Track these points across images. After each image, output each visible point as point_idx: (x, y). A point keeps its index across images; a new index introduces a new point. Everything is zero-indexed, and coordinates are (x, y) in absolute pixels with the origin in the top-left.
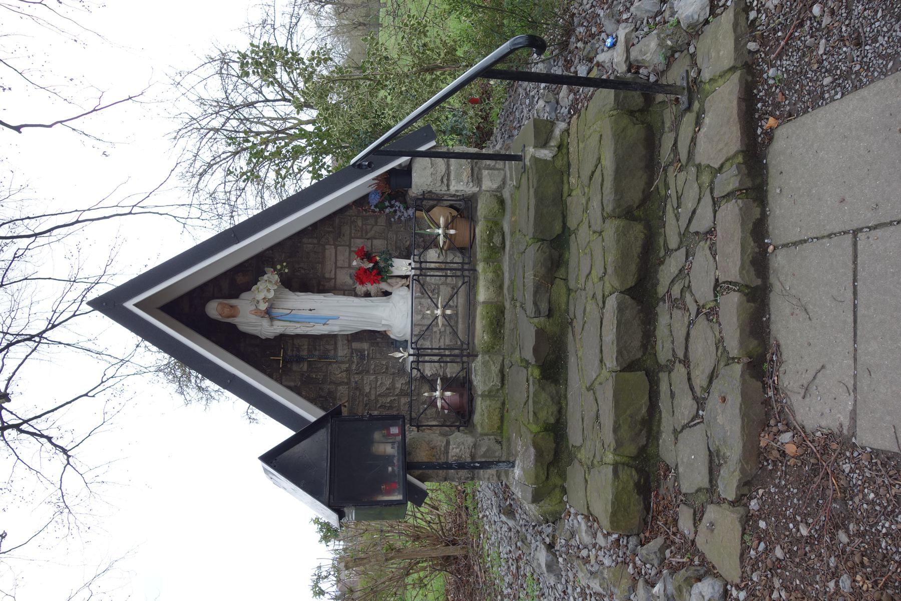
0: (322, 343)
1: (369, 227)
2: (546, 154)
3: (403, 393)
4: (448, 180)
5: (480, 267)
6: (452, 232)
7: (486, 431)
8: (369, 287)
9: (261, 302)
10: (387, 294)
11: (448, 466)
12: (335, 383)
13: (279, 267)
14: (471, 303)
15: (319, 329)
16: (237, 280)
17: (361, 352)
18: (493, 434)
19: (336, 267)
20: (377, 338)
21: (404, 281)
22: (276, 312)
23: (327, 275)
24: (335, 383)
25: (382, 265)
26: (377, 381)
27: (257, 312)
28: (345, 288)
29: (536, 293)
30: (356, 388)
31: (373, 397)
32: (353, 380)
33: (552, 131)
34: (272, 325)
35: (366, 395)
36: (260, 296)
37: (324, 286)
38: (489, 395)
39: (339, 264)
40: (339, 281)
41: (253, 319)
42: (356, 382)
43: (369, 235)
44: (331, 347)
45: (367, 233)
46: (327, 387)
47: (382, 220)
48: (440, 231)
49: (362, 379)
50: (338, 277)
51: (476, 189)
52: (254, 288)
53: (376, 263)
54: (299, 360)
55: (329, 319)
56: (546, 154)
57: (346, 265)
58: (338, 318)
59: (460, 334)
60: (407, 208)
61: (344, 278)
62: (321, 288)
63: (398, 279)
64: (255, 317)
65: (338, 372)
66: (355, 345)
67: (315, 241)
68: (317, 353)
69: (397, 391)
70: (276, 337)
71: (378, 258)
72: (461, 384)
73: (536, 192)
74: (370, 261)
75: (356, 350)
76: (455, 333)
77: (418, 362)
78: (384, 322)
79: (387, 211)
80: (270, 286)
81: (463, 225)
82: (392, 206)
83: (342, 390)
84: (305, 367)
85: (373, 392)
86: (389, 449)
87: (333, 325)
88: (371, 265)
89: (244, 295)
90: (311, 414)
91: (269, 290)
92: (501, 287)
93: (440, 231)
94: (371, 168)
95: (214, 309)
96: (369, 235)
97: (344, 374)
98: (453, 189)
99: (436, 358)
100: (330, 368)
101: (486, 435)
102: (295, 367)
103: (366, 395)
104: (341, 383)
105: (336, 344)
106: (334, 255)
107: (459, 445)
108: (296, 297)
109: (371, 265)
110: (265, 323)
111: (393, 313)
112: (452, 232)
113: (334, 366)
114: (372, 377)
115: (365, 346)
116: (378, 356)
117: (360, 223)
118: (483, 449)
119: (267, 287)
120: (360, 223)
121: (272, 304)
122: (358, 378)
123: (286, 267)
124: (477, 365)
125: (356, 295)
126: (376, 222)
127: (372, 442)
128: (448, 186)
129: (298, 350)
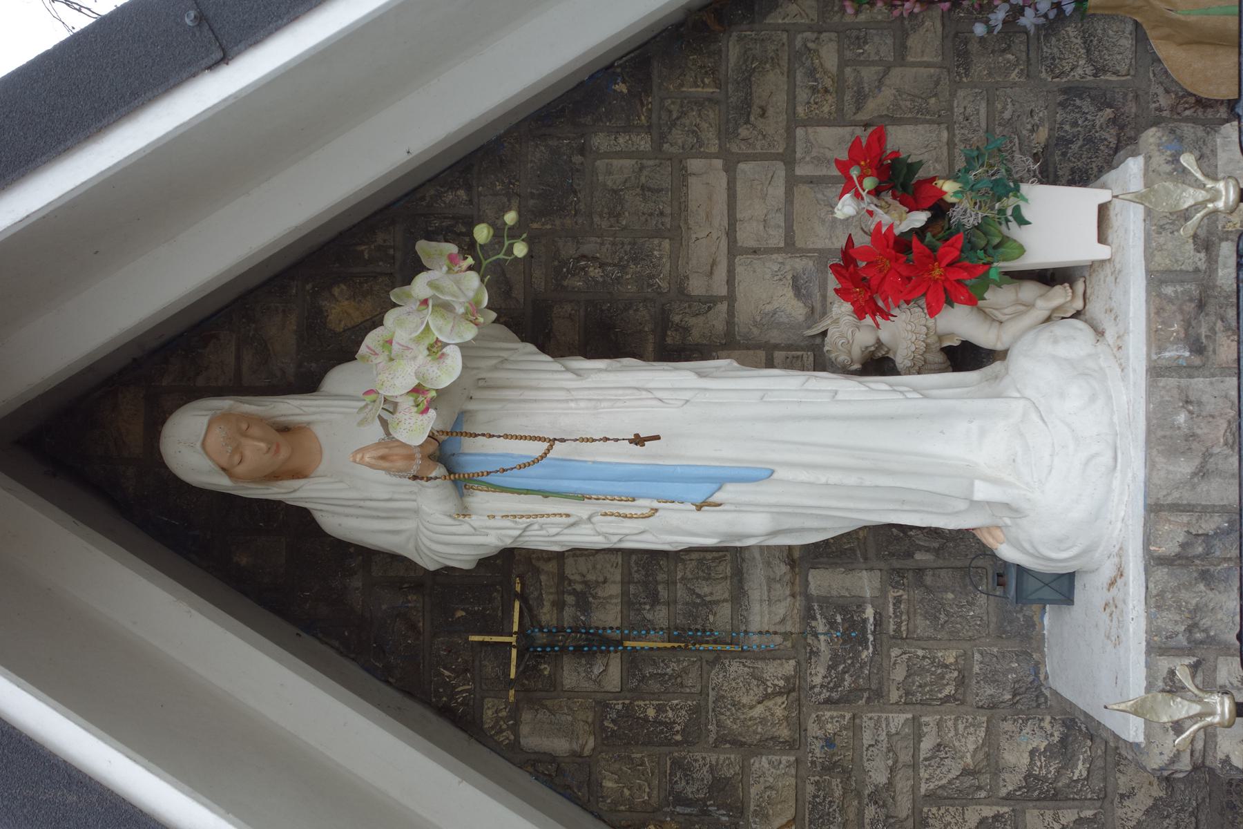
0: (685, 590)
1: (869, 74)
8: (905, 328)
9: (407, 403)
10: (964, 356)
12: (737, 744)
13: (482, 233)
15: (677, 527)
16: (298, 314)
17: (846, 614)
21: (1059, 295)
22: (481, 451)
23: (696, 286)
24: (737, 744)
25: (967, 213)
26: (918, 737)
27: (388, 454)
28: (775, 336)
31: (903, 807)
32: (813, 729)
34: (464, 512)
35: (875, 798)
37: (686, 330)
39: (746, 236)
41: (381, 485)
42: (829, 742)
43: (872, 108)
44: (720, 591)
45: (860, 99)
49: (855, 727)
50: (740, 290)
52: (372, 339)
53: (940, 209)
54: (593, 644)
55: (721, 482)
57: (776, 238)
58: (763, 475)
61: (766, 293)
62: (672, 338)
63: (1029, 290)
64: (381, 475)
65: (749, 697)
66: (821, 581)
67: (643, 143)
68: (660, 616)
69: (1011, 782)
70: (484, 563)
71: (949, 187)
74: (913, 205)
75: (825, 601)
78: (982, 492)
80: (442, 329)
83: (771, 775)
84: (612, 673)
85: (903, 785)
87: (740, 507)
88: (919, 218)
89: (340, 378)
91: (436, 349)
95: (197, 444)
96: (872, 108)
97: (778, 707)
100: (716, 677)
102: (571, 675)
103: (875, 798)
104: (766, 745)
106: (721, 197)
108: (568, 380)
109: (919, 218)
113: (735, 668)
114: (898, 720)
116: (922, 625)
117: (829, 57)
119: (427, 333)
120: (829, 57)
121: (462, 416)
122: (834, 720)
123: (514, 233)
126: (901, 50)
129: (583, 603)
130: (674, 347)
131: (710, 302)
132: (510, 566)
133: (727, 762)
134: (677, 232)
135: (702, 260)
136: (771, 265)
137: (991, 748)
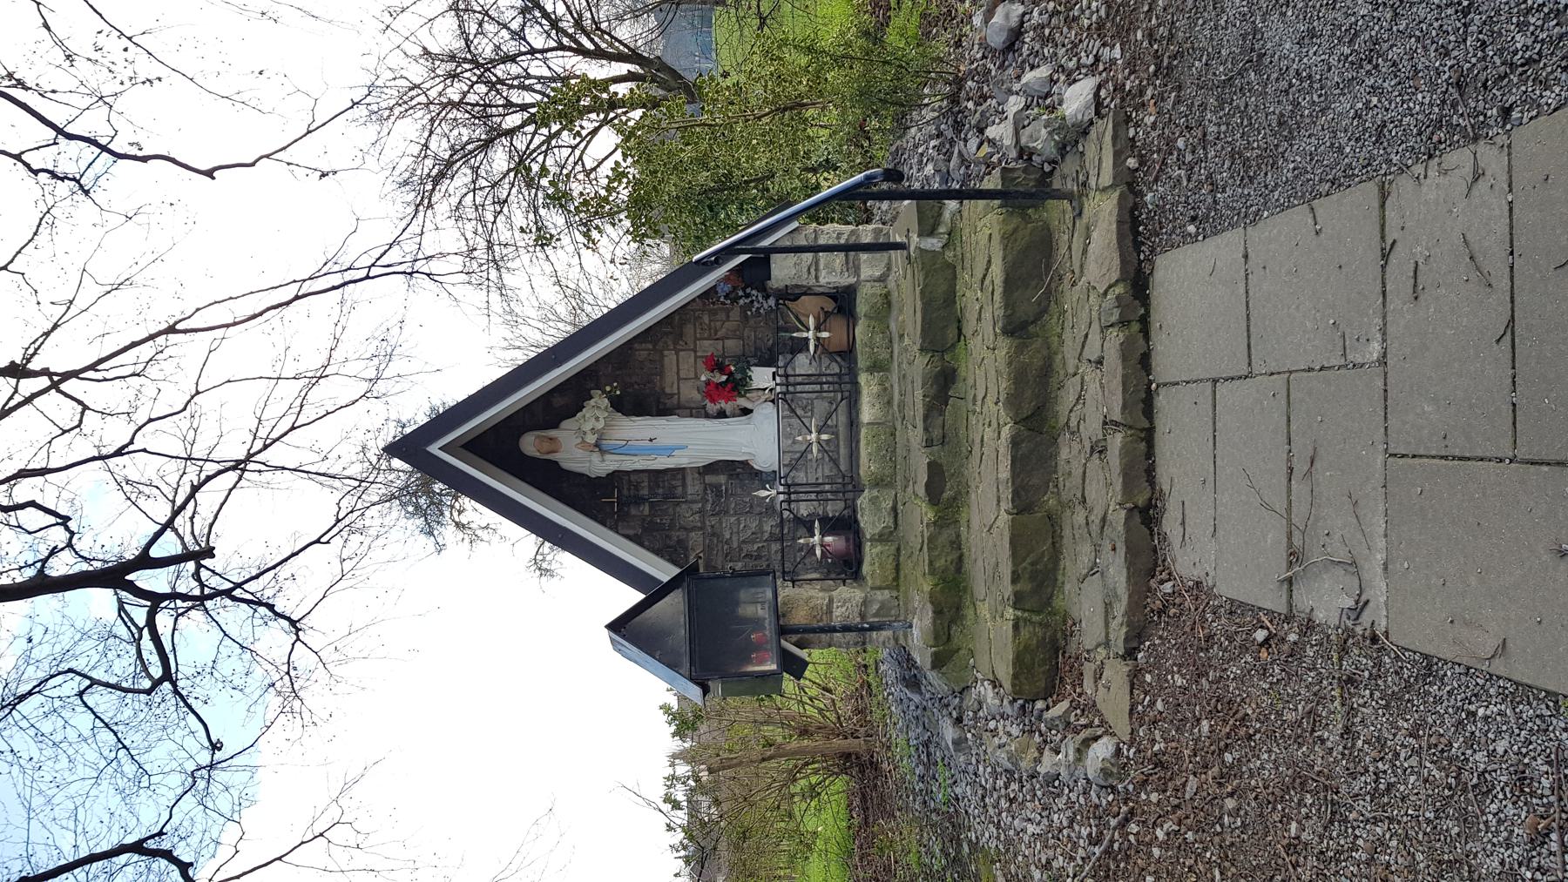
0: (666, 481)
2: (933, 243)
3: (773, 538)
4: (817, 270)
5: (863, 378)
6: (825, 335)
7: (878, 583)
10: (746, 412)
11: (833, 630)
14: (853, 423)
17: (716, 488)
18: (887, 588)
19: (679, 379)
20: (739, 471)
23: (668, 390)
29: (926, 418)
30: (714, 534)
31: (735, 545)
33: (940, 215)
36: (587, 427)
38: (881, 538)
40: (683, 398)
41: (579, 453)
43: (720, 334)
44: (679, 483)
46: (675, 535)
47: (735, 314)
48: (810, 334)
51: (852, 280)
53: (730, 374)
54: (638, 501)
56: (933, 243)
59: (843, 468)
60: (767, 297)
61: (690, 393)
65: (688, 514)
66: (709, 479)
69: (766, 536)
72: (846, 524)
73: (922, 292)
74: (722, 371)
76: (835, 462)
77: (789, 501)
78: (744, 450)
79: (741, 302)
80: (598, 413)
81: (839, 323)
82: (747, 296)
84: (646, 509)
85: (735, 538)
86: (762, 612)
89: (565, 424)
90: (663, 571)
91: (597, 419)
92: (889, 403)
93: (810, 334)
95: (530, 444)
96: (720, 334)
97: (697, 517)
98: (822, 281)
99: (813, 496)
101: (880, 588)
102: (633, 511)
104: (693, 529)
105: (684, 478)
107: (846, 600)
109: (724, 378)
110: (596, 457)
111: (755, 438)
112: (825, 335)
114: (733, 519)
115: (722, 479)
116: (739, 491)
117: (706, 319)
118: (876, 607)
119: (596, 413)
120: (706, 319)
122: (714, 521)
124: (863, 501)
125: (707, 416)
127: (737, 603)
128: (817, 278)
130: (663, 411)
131: (672, 395)
132: (616, 476)
133: (682, 535)
134: (661, 374)
135: (670, 383)
136: (690, 383)
137: (760, 526)
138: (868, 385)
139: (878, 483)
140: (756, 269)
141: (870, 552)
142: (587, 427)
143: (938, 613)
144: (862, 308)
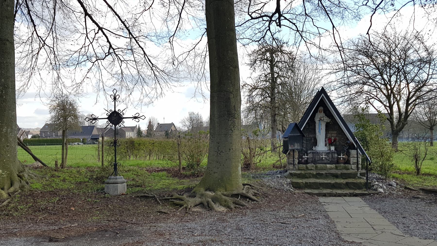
0: (314, 131)
2: (359, 175)
8: (327, 142)
10: (326, 145)
14: (325, 164)
15: (317, 131)
36: (324, 118)
41: (319, 116)
47: (343, 144)
56: (359, 175)
61: (329, 135)
76: (318, 161)
81: (343, 162)
92: (330, 169)
94: (354, 141)
95: (321, 108)
107: (296, 161)
110: (319, 119)
111: (321, 147)
119: (327, 119)
124: (313, 164)
132: (315, 123)
138: (333, 166)
139: (316, 167)
140: (352, 147)
141: (304, 166)
142: (324, 118)
143: (299, 174)
144: (346, 165)
